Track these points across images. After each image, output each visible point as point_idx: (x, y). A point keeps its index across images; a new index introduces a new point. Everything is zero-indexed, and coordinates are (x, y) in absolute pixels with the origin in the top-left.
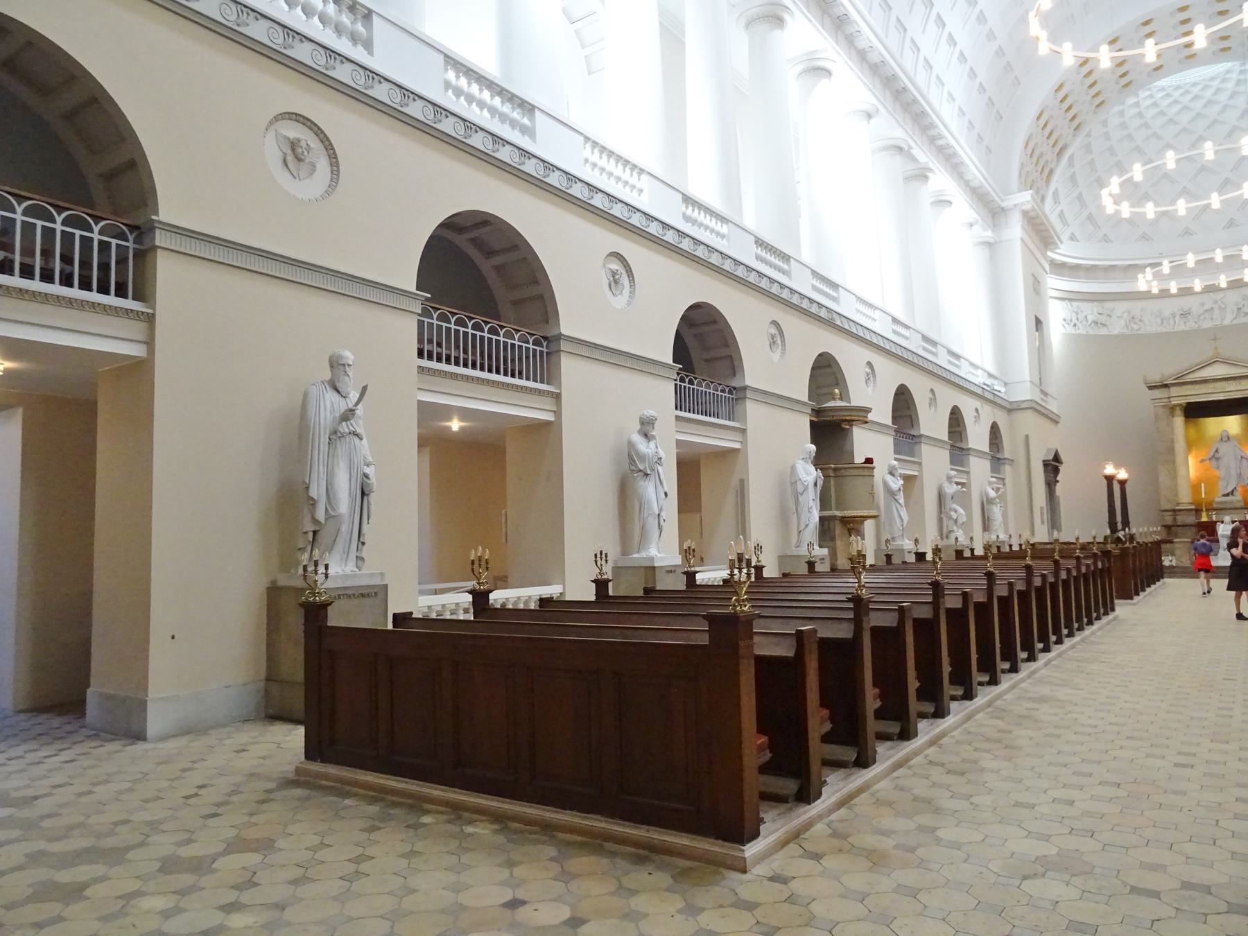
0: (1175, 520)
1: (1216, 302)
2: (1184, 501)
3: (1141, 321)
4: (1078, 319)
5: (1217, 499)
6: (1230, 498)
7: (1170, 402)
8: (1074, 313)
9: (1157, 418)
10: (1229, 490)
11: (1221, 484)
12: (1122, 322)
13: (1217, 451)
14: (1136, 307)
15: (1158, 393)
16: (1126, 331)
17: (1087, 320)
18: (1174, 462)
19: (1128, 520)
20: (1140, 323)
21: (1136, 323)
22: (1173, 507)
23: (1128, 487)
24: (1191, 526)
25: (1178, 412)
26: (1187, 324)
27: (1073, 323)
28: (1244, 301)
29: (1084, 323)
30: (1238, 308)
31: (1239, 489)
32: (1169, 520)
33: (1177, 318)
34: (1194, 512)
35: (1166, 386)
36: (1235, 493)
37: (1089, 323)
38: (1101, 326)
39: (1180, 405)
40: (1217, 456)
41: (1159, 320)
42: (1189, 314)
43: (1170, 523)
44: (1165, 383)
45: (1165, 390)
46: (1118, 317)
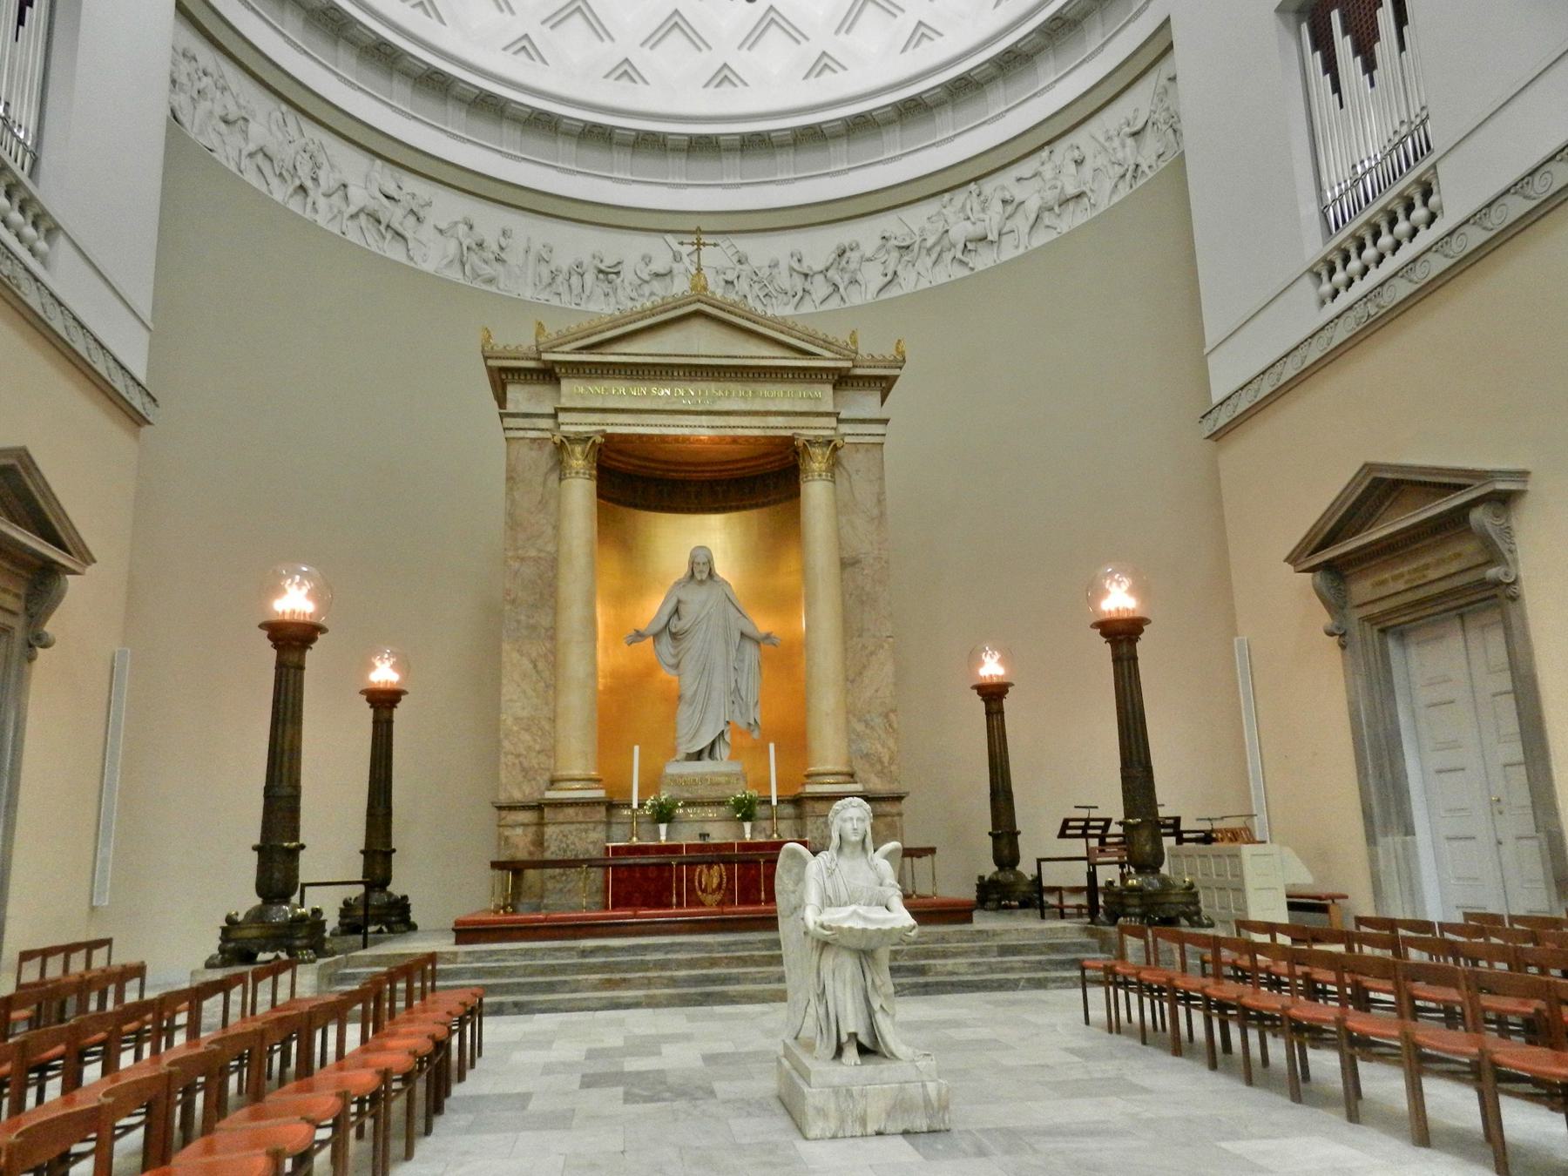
0: (539, 842)
1: (677, 258)
2: (577, 772)
3: (497, 260)
4: (315, 180)
5: (673, 769)
6: (705, 766)
7: (559, 425)
8: (306, 156)
10: (704, 742)
11: (684, 712)
12: (452, 248)
13: (676, 611)
14: (490, 220)
15: (520, 397)
16: (454, 274)
17: (346, 198)
18: (552, 634)
19: (389, 843)
20: (498, 266)
21: (486, 262)
22: (537, 796)
23: (399, 713)
24: (591, 863)
25: (578, 461)
26: (612, 300)
27: (297, 183)
28: (743, 267)
29: (337, 199)
31: (727, 737)
32: (520, 843)
33: (589, 278)
34: (601, 813)
35: (548, 374)
36: (723, 751)
37: (353, 209)
38: (389, 235)
39: (584, 439)
40: (676, 626)
41: (545, 271)
42: (618, 273)
43: (522, 855)
44: (547, 357)
45: (544, 390)
46: (441, 231)
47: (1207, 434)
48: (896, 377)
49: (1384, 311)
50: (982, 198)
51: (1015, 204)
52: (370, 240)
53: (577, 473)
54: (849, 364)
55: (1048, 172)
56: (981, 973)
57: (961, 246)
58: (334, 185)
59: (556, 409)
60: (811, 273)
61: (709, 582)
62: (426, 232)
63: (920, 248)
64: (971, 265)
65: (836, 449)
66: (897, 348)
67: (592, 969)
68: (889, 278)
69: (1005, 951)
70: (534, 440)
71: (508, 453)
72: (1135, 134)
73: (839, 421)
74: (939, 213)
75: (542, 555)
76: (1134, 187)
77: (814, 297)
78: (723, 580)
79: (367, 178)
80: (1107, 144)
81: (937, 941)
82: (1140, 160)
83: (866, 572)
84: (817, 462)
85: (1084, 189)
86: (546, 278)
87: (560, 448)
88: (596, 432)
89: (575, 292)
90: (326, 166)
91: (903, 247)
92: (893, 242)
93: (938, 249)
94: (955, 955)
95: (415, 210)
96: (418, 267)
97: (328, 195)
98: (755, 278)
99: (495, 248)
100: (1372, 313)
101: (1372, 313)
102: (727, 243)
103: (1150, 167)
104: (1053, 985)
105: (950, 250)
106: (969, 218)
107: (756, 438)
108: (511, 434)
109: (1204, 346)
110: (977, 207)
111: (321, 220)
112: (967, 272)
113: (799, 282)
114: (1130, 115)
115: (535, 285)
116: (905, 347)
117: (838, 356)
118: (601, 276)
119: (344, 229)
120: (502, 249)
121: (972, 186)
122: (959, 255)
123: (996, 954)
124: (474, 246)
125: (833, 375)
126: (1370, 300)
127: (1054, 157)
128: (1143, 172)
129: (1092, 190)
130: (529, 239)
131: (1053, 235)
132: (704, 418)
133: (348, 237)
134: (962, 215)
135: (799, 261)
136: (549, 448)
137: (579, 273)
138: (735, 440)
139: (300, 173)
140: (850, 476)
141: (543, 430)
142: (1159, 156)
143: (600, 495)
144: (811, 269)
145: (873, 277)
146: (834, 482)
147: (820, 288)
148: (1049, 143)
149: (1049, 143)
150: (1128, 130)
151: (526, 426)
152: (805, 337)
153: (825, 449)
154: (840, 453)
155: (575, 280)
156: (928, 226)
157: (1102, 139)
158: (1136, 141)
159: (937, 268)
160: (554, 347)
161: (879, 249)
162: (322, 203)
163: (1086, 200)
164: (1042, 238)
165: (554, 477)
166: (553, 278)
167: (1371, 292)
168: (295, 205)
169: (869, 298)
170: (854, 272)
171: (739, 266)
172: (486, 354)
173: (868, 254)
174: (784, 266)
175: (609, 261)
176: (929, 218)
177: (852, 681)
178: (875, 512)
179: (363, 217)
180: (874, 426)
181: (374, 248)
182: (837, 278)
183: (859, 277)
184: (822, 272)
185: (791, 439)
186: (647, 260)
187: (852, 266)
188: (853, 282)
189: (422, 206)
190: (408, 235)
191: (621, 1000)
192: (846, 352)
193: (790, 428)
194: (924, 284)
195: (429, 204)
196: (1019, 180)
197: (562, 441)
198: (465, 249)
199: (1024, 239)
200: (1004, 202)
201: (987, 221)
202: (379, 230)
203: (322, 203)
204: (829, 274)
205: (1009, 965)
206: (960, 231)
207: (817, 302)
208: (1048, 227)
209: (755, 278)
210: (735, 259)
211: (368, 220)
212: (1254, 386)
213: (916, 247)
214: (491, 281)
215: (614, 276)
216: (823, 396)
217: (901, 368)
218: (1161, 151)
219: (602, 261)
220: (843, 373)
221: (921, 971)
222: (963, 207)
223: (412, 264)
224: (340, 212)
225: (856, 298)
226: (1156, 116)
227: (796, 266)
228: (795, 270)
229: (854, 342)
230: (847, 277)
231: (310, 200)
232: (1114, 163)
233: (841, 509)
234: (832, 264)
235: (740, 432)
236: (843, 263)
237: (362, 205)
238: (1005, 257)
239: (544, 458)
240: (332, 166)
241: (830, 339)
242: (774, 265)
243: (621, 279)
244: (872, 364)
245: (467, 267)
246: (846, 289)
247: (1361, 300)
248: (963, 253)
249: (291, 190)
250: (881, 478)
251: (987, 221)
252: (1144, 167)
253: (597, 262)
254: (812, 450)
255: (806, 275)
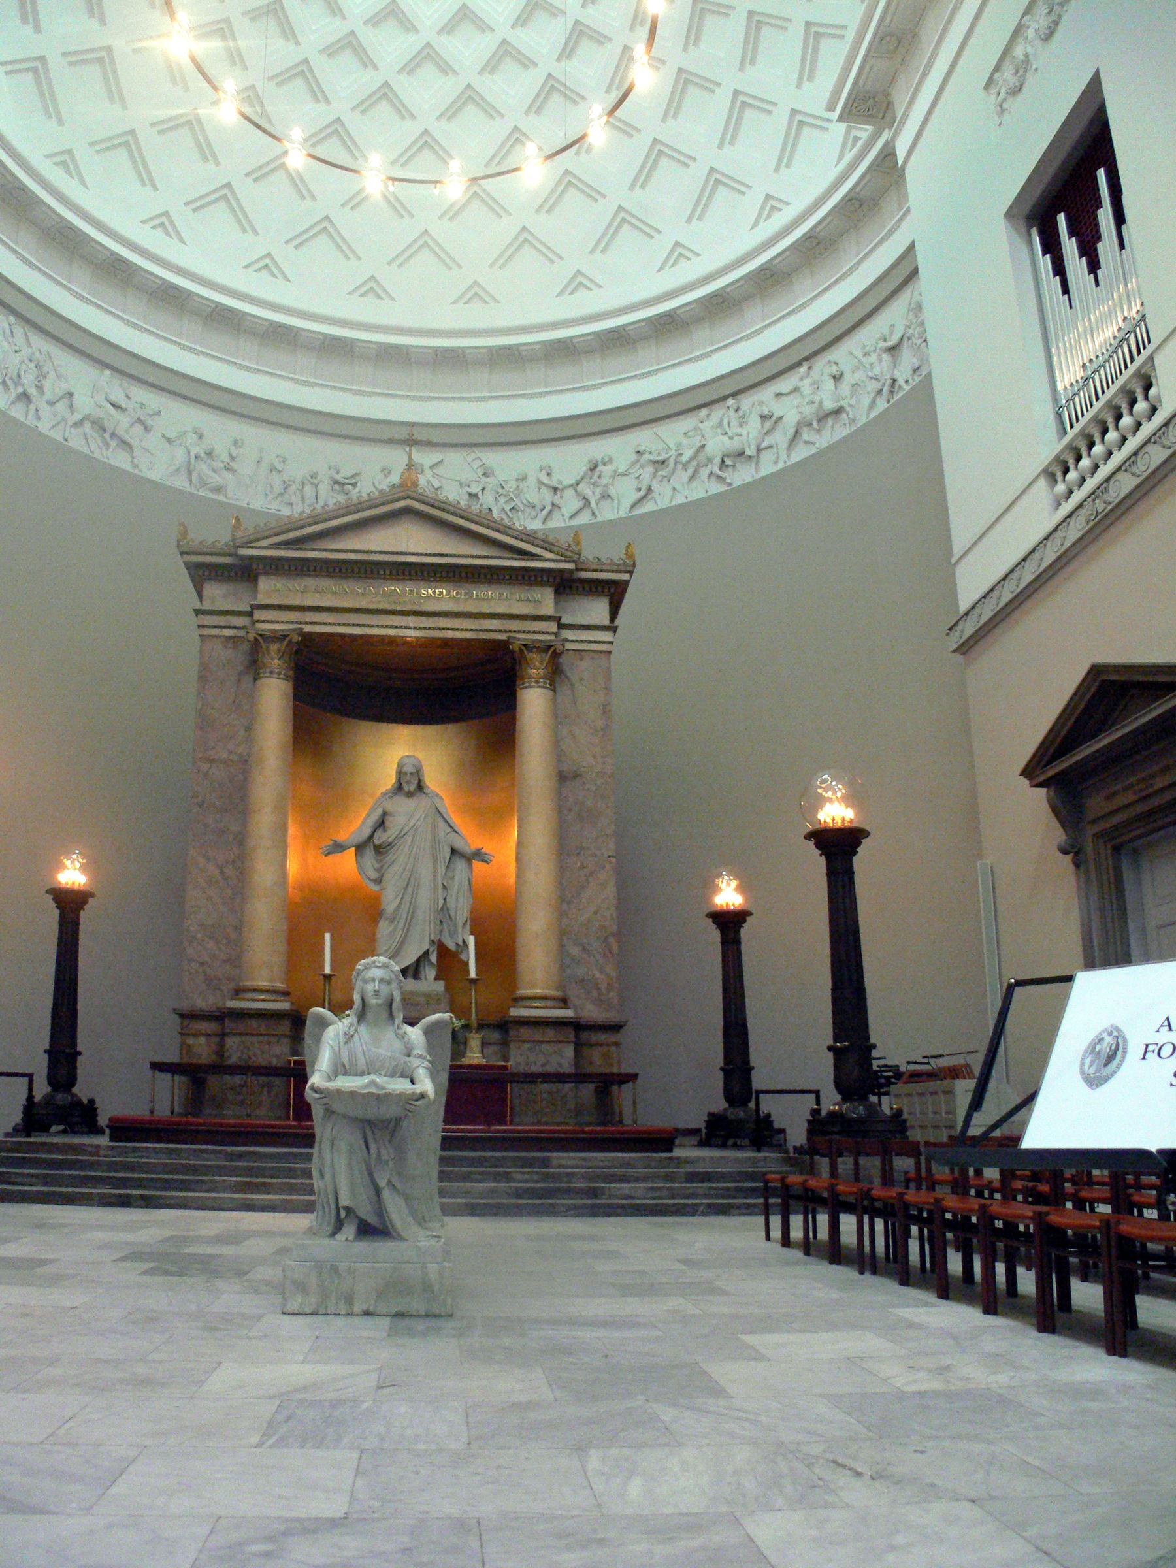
3: (228, 469)
4: (40, 388)
7: (254, 623)
9: (203, 678)
12: (180, 454)
15: (218, 595)
16: (180, 483)
17: (71, 406)
20: (228, 475)
21: (214, 471)
28: (488, 480)
29: (61, 407)
30: (471, 495)
37: (77, 417)
38: (113, 443)
39: (281, 637)
41: (276, 480)
42: (354, 485)
45: (241, 588)
46: (169, 441)
47: (955, 646)
48: (626, 583)
49: (1110, 507)
50: (740, 413)
51: (773, 419)
52: (93, 446)
53: (271, 672)
54: (571, 566)
55: (806, 386)
56: (660, 1198)
57: (718, 460)
58: (59, 392)
59: (252, 606)
60: (560, 487)
61: (418, 794)
62: (153, 441)
63: (676, 463)
64: (728, 480)
65: (556, 655)
66: (627, 551)
67: (234, 1172)
68: (642, 493)
69: (692, 1177)
70: (230, 638)
71: (201, 652)
72: (891, 350)
73: (561, 626)
74: (696, 429)
75: (231, 757)
76: (892, 401)
77: (564, 510)
78: (433, 792)
79: (95, 389)
80: (864, 360)
81: (621, 1166)
82: (897, 375)
83: (587, 786)
84: (536, 668)
85: (842, 403)
86: (278, 489)
87: (255, 645)
88: (294, 630)
89: (308, 502)
90: (52, 375)
91: (657, 462)
92: (647, 457)
93: (694, 463)
94: (637, 1180)
95: (142, 418)
96: (144, 475)
97: (52, 403)
98: (501, 491)
99: (227, 459)
100: (1100, 510)
101: (1100, 510)
102: (473, 456)
103: (906, 382)
104: (738, 1211)
105: (707, 465)
106: (726, 433)
107: (469, 640)
108: (206, 632)
109: (951, 554)
110: (734, 423)
111: (44, 426)
112: (724, 488)
113: (548, 496)
114: (886, 331)
115: (266, 495)
116: (636, 551)
117: (559, 557)
118: (336, 487)
119: (67, 435)
120: (233, 458)
121: (730, 402)
122: (716, 470)
123: (683, 1180)
124: (203, 455)
125: (555, 578)
126: (1098, 497)
127: (812, 373)
128: (900, 386)
129: (851, 406)
130: (261, 450)
131: (813, 450)
132: (410, 618)
133: (71, 444)
134: (719, 431)
135: (549, 474)
136: (246, 647)
137: (312, 484)
138: (446, 643)
139: (24, 380)
140: (572, 685)
141: (238, 628)
142: (915, 371)
143: (296, 697)
144: (561, 483)
145: (626, 492)
146: (554, 690)
147: (570, 503)
148: (806, 359)
149: (806, 359)
150: (882, 344)
151: (223, 624)
152: (524, 537)
153: (544, 655)
154: (563, 660)
155: (308, 489)
156: (685, 441)
157: (860, 355)
158: (893, 356)
159: (694, 484)
160: (258, 540)
161: (633, 464)
162: (45, 410)
163: (844, 415)
164: (801, 453)
165: (248, 679)
166: (285, 489)
167: (1098, 488)
168: (17, 412)
169: (623, 513)
170: (606, 486)
171: (484, 479)
172: (182, 550)
173: (622, 469)
174: (532, 480)
175: (346, 472)
176: (685, 433)
177: (569, 903)
178: (600, 724)
179: (87, 425)
180: (600, 633)
181: (97, 455)
182: (588, 492)
183: (612, 491)
184: (571, 486)
185: (506, 643)
186: (386, 472)
187: (604, 481)
188: (606, 496)
189: (151, 416)
190: (134, 443)
191: (257, 1203)
192: (569, 554)
193: (506, 631)
194: (680, 500)
195: (158, 413)
196: (778, 395)
197: (256, 639)
198: (193, 457)
199: (784, 455)
200: (763, 417)
201: (744, 438)
202: (103, 437)
203: (45, 410)
204: (579, 488)
205: (691, 1191)
206: (717, 445)
207: (567, 515)
208: (806, 442)
209: (501, 491)
210: (480, 472)
211: (93, 428)
212: (996, 594)
213: (671, 462)
214: (219, 489)
215: (350, 487)
216: (545, 600)
217: (631, 573)
218: (916, 365)
219: (338, 473)
220: (566, 576)
221: (594, 1193)
222: (720, 424)
223: (136, 472)
224: (64, 420)
225: (608, 513)
226: (911, 331)
227: (546, 480)
228: (543, 484)
229: (578, 543)
230: (598, 491)
231: (32, 407)
232: (871, 378)
233: (558, 718)
234: (582, 478)
235: (450, 634)
236: (595, 477)
237: (87, 412)
238: (764, 472)
239: (237, 657)
240: (59, 377)
241: (551, 539)
242: (523, 478)
243: (357, 490)
244: (599, 567)
245: (194, 477)
246: (597, 504)
247: (1089, 497)
248: (720, 469)
249: (13, 396)
250: (607, 689)
251: (744, 438)
252: (901, 382)
253: (333, 472)
254: (530, 656)
255: (555, 489)
